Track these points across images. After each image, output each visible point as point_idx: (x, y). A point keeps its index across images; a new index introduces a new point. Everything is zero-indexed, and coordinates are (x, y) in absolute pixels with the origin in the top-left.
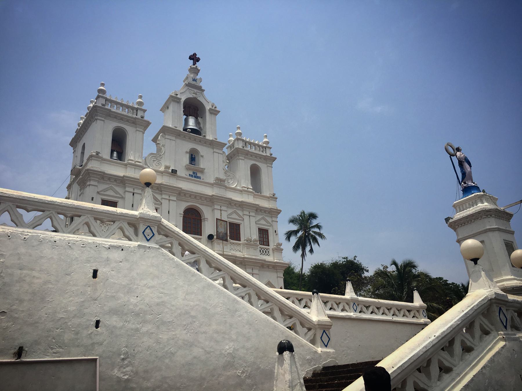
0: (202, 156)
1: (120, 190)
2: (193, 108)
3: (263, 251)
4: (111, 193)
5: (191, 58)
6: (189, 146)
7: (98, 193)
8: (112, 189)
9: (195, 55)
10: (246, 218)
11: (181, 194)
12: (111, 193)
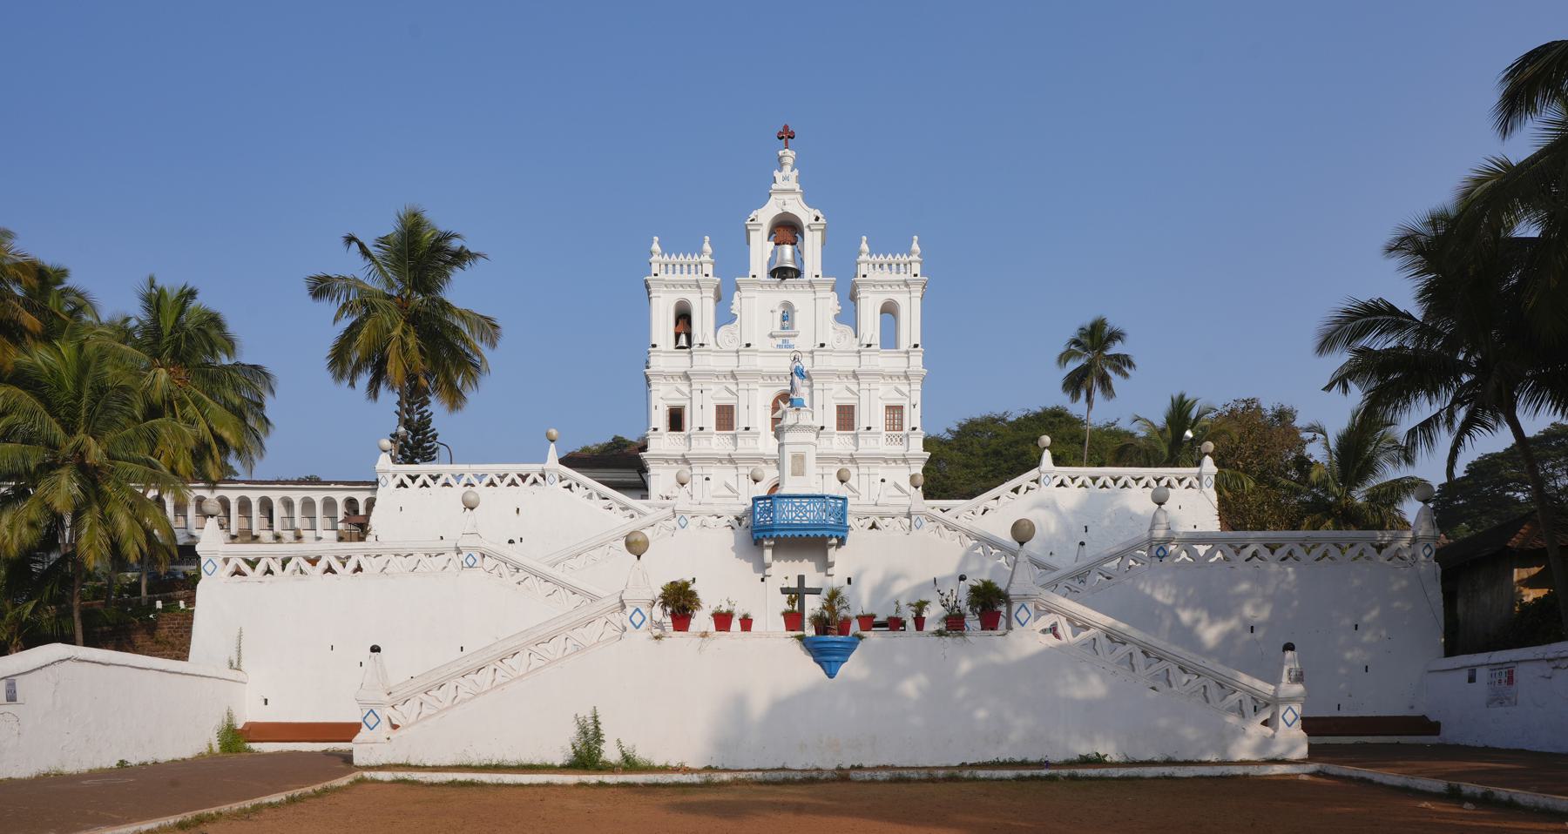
1: (685, 388)
9: (786, 127)
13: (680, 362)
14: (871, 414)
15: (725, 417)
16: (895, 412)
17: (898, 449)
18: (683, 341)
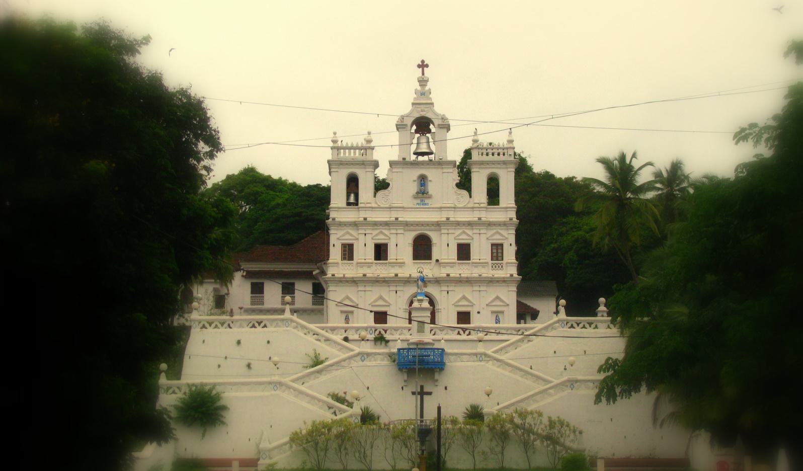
0: (430, 181)
2: (423, 125)
3: (495, 267)
4: (347, 237)
5: (419, 66)
6: (416, 173)
7: (338, 239)
8: (348, 233)
9: (423, 61)
10: (476, 237)
11: (407, 225)
12: (347, 237)
13: (350, 215)
14: (481, 251)
15: (381, 252)
16: (497, 251)
17: (499, 274)
18: (352, 199)
